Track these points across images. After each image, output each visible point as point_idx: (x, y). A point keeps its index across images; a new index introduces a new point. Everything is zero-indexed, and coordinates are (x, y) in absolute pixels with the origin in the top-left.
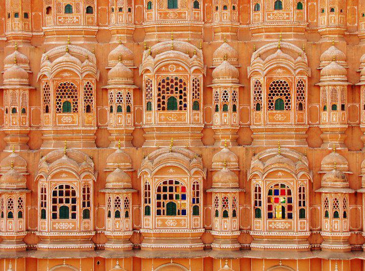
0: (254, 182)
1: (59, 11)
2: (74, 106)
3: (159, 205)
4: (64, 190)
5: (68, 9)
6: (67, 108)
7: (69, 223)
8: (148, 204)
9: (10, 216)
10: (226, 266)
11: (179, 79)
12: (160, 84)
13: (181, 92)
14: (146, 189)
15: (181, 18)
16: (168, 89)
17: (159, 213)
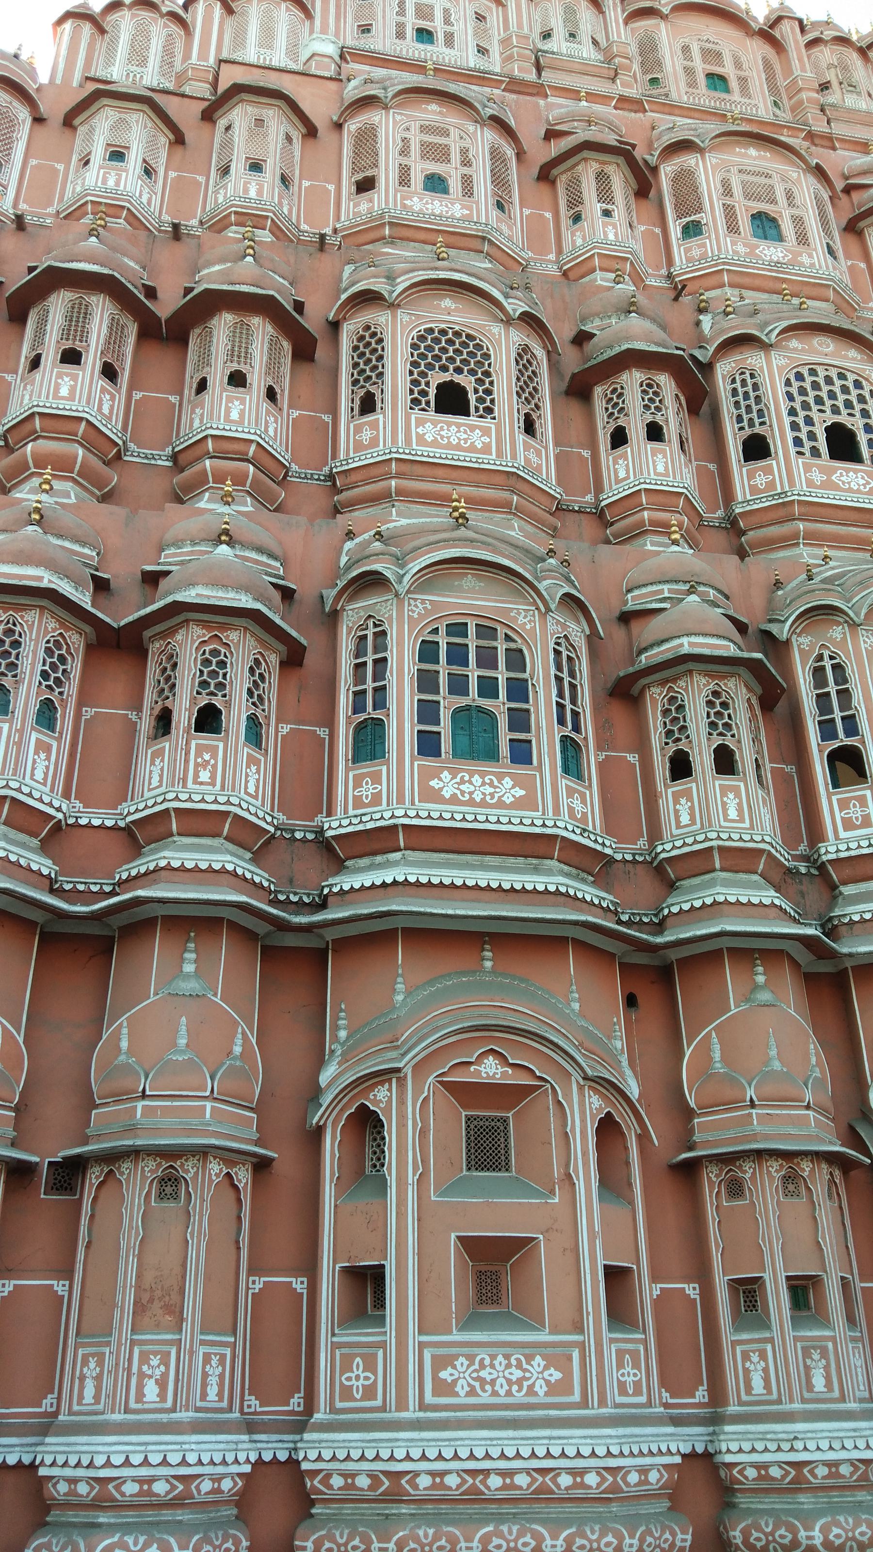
2: (481, 400)
5: (436, 184)
7: (500, 777)
8: (843, 740)
11: (851, 377)
15: (801, 264)
16: (819, 401)
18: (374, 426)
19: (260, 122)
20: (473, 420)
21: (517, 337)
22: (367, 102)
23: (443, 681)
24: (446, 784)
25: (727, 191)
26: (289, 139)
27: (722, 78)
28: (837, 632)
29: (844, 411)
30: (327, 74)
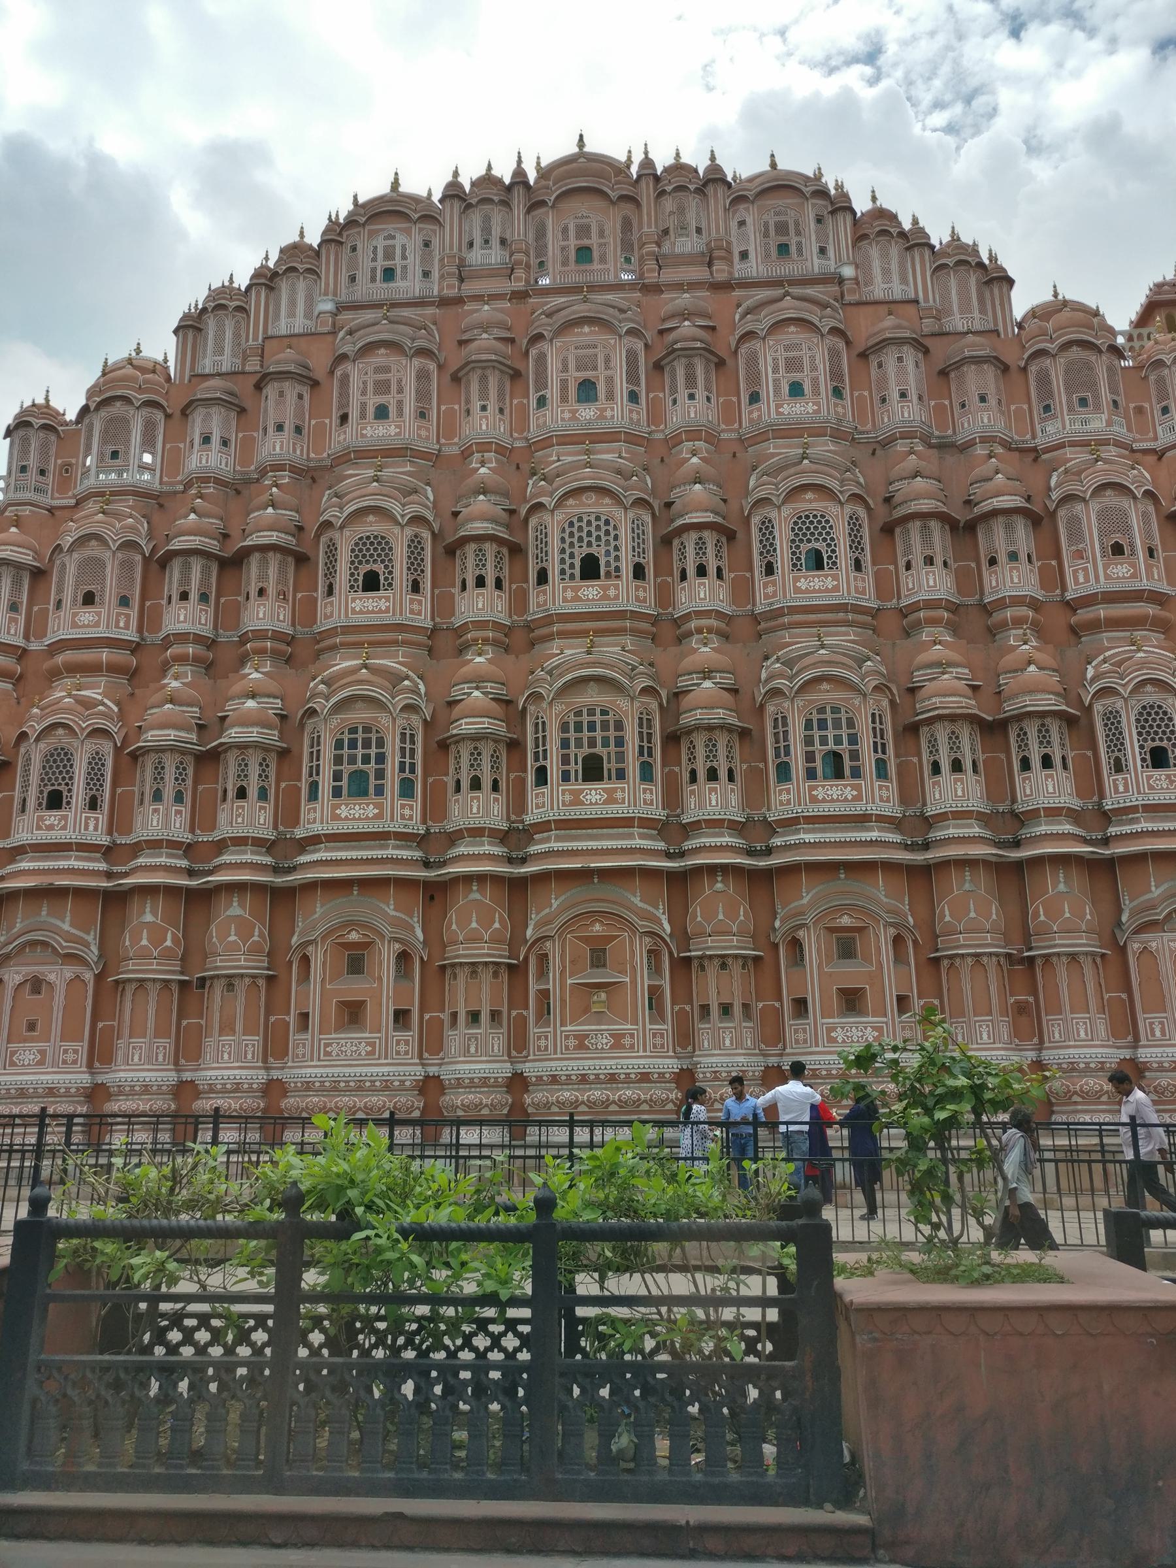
0: (770, 709)
1: (363, 416)
2: (386, 579)
3: (565, 760)
4: (360, 736)
5: (382, 413)
6: (371, 583)
8: (543, 763)
9: (242, 793)
10: (719, 886)
11: (603, 518)
12: (563, 531)
13: (608, 543)
14: (537, 732)
16: (580, 539)
17: (566, 777)
18: (331, 603)
19: (281, 394)
20: (381, 593)
21: (409, 532)
22: (343, 357)
23: (345, 759)
24: (343, 812)
25: (565, 368)
26: (300, 397)
27: (588, 249)
28: (544, 705)
29: (594, 543)
30: (325, 329)
